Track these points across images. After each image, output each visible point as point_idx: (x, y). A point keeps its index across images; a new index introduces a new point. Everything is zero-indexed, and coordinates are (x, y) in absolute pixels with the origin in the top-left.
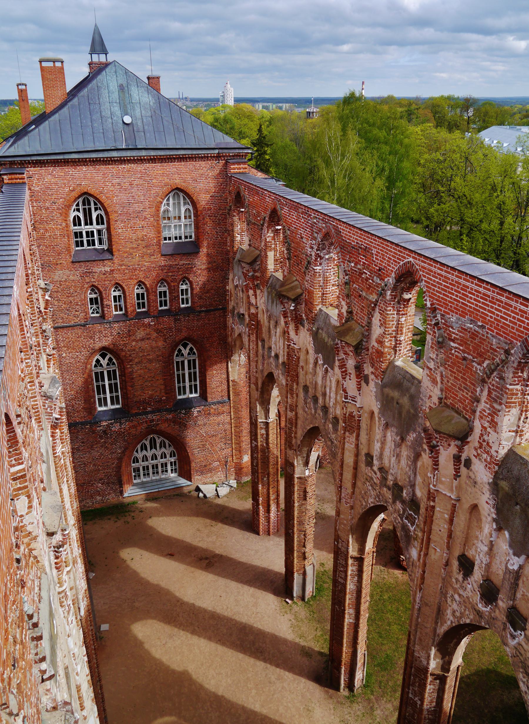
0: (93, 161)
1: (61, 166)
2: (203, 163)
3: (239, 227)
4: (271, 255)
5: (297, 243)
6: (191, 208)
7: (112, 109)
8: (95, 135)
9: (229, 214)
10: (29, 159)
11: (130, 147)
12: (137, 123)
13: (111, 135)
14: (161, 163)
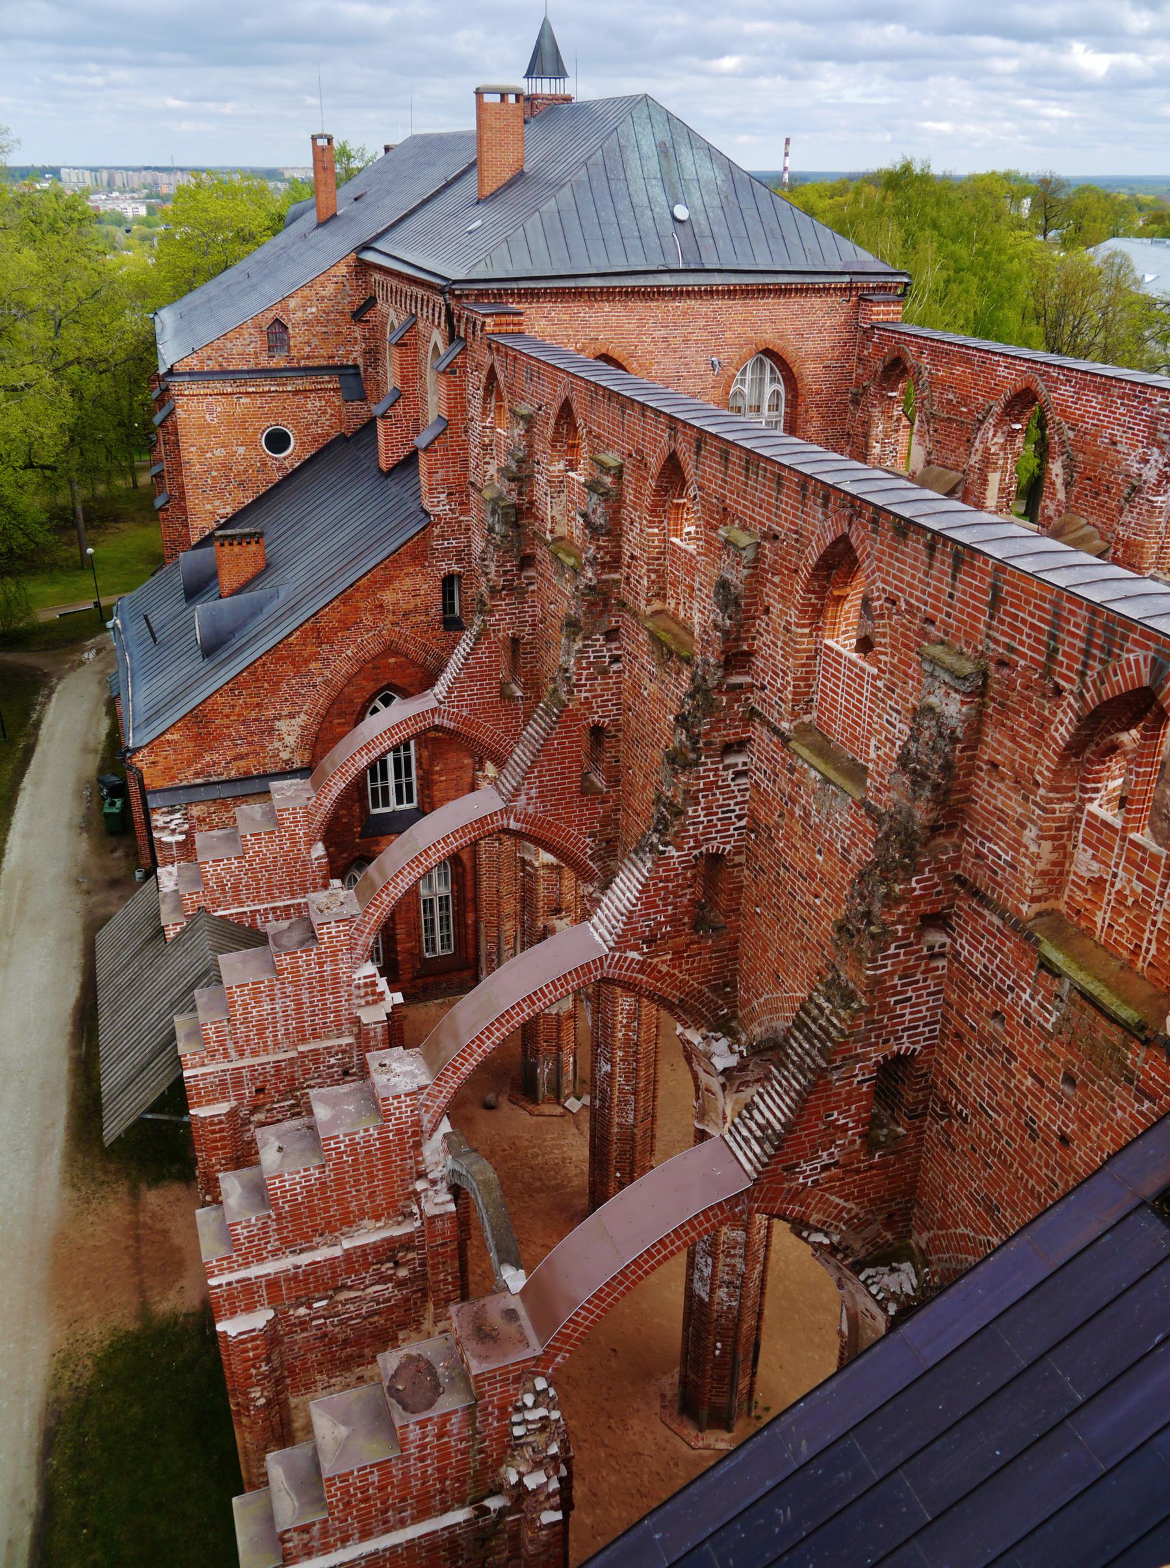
0: (627, 293)
1: (567, 302)
2: (816, 302)
3: (880, 428)
4: (994, 479)
5: (1100, 456)
6: (781, 388)
7: (650, 192)
8: (626, 241)
9: (856, 402)
10: (514, 285)
11: (692, 267)
12: (697, 219)
13: (653, 242)
14: (745, 298)
